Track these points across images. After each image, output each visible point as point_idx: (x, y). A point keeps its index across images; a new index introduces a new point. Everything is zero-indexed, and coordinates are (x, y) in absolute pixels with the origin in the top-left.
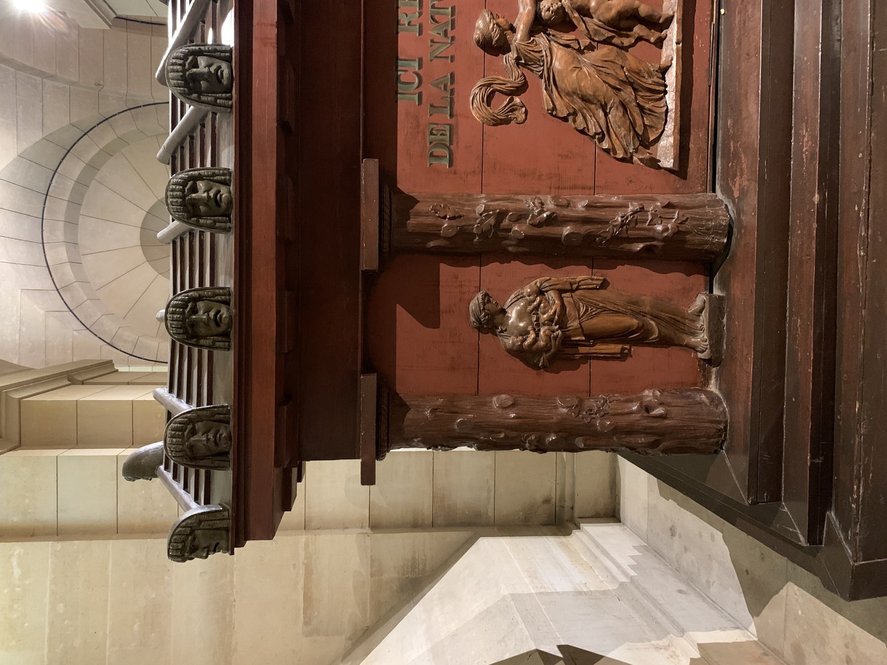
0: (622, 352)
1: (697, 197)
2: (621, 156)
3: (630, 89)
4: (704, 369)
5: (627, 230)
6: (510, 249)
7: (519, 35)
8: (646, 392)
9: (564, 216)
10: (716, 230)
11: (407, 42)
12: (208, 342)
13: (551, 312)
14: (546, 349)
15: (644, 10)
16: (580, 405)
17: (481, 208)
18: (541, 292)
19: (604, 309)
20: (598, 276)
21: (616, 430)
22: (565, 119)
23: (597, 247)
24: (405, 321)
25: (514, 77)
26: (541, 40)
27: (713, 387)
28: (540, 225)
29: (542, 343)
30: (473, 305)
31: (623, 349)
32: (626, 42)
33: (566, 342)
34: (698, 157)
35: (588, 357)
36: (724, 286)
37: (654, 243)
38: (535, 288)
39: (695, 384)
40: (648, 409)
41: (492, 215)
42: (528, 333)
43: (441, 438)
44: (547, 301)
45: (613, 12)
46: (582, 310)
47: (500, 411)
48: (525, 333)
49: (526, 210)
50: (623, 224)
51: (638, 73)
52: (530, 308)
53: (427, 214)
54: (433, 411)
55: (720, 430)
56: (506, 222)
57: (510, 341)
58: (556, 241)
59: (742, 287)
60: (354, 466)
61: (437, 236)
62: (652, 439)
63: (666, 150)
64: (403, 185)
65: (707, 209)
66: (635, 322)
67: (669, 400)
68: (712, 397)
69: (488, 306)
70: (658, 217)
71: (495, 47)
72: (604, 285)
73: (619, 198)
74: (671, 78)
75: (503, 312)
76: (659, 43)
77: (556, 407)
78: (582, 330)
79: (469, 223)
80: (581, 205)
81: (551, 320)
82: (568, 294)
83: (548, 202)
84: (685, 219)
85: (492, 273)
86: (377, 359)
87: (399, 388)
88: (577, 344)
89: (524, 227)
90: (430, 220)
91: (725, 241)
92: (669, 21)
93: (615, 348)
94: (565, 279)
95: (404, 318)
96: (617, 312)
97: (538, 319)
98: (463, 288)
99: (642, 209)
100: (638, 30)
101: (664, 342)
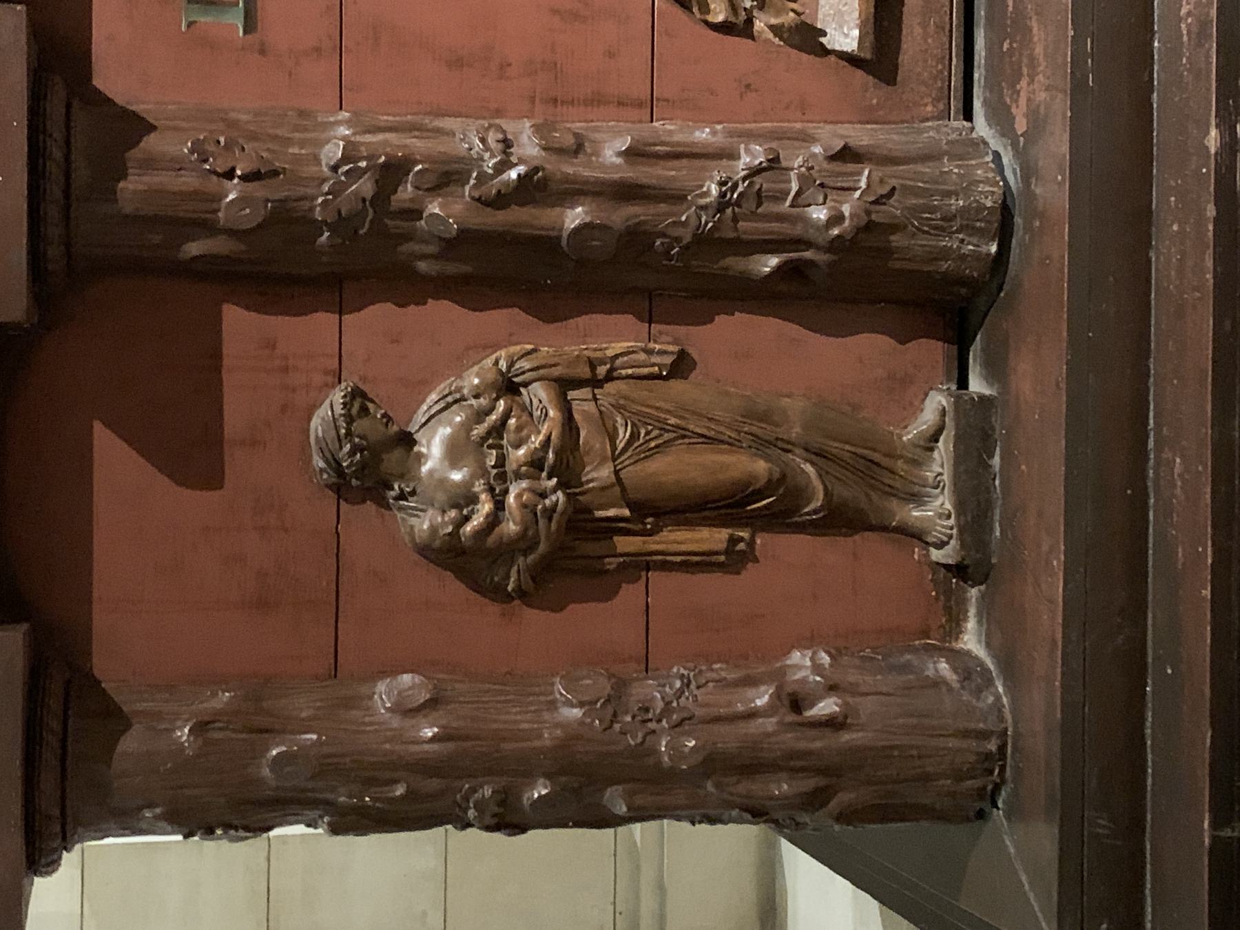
0: (728, 552)
1: (921, 132)
2: (721, 18)
4: (948, 593)
5: (735, 219)
6: (422, 266)
8: (796, 657)
9: (567, 179)
10: (968, 222)
13: (536, 441)
14: (525, 543)
16: (616, 698)
17: (333, 151)
18: (509, 386)
19: (682, 433)
20: (664, 344)
21: (714, 764)
23: (660, 264)
27: (971, 640)
28: (500, 201)
29: (511, 527)
30: (317, 425)
31: (733, 541)
33: (581, 523)
34: (924, 26)
35: (641, 565)
36: (996, 370)
37: (808, 254)
38: (491, 376)
39: (926, 634)
40: (797, 703)
41: (364, 171)
42: (473, 500)
43: (224, 804)
44: (527, 410)
46: (623, 435)
47: (396, 722)
48: (464, 500)
49: (460, 160)
50: (722, 204)
52: (479, 430)
53: (178, 166)
54: (200, 728)
55: (988, 756)
56: (406, 192)
57: (425, 522)
59: (1034, 373)
61: (207, 227)
64: (113, 77)
65: (947, 165)
66: (761, 467)
67: (852, 677)
68: (966, 666)
69: (360, 426)
72: (681, 366)
73: (714, 133)
75: (407, 440)
77: (552, 705)
79: (302, 191)
80: (611, 152)
81: (536, 464)
82: (585, 392)
83: (524, 138)
84: (885, 190)
85: (373, 332)
87: (103, 666)
88: (611, 528)
89: (458, 207)
90: (188, 181)
91: (994, 248)
93: (713, 538)
94: (574, 350)
95: (115, 462)
96: (709, 440)
97: (501, 462)
98: (291, 375)
99: (774, 163)
101: (839, 520)
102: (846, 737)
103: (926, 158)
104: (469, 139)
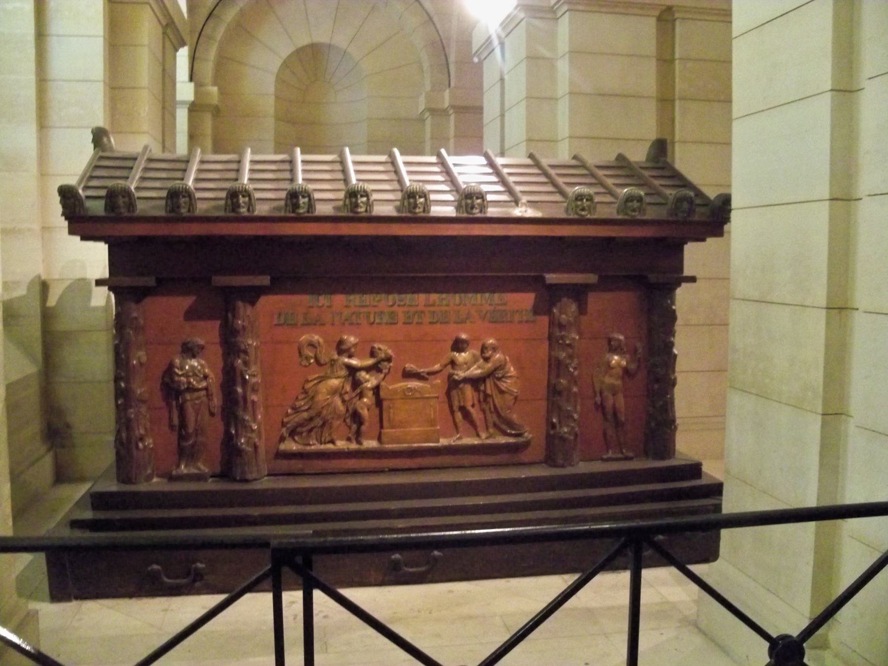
3: (321, 423)
7: (346, 360)
10: (243, 472)
11: (339, 299)
12: (169, 202)
14: (173, 381)
15: (363, 428)
16: (144, 402)
17: (250, 342)
18: (206, 377)
21: (129, 420)
22: (303, 388)
24: (185, 302)
25: (324, 359)
26: (344, 372)
29: (176, 378)
32: (348, 421)
40: (142, 439)
44: (201, 381)
45: (361, 411)
46: (197, 402)
50: (244, 420)
51: (331, 428)
54: (136, 318)
56: (242, 355)
57: (177, 361)
58: (234, 384)
60: (106, 274)
62: (125, 441)
63: (291, 446)
66: (191, 430)
70: (249, 439)
71: (341, 349)
72: (212, 414)
74: (330, 446)
76: (349, 439)
78: (185, 401)
80: (254, 397)
81: (189, 383)
85: (216, 351)
86: (165, 285)
88: (177, 399)
92: (359, 443)
93: (176, 421)
98: (207, 334)
99: (253, 431)
100: (354, 427)
102: (134, 448)
103: (258, 466)
104: (253, 369)
